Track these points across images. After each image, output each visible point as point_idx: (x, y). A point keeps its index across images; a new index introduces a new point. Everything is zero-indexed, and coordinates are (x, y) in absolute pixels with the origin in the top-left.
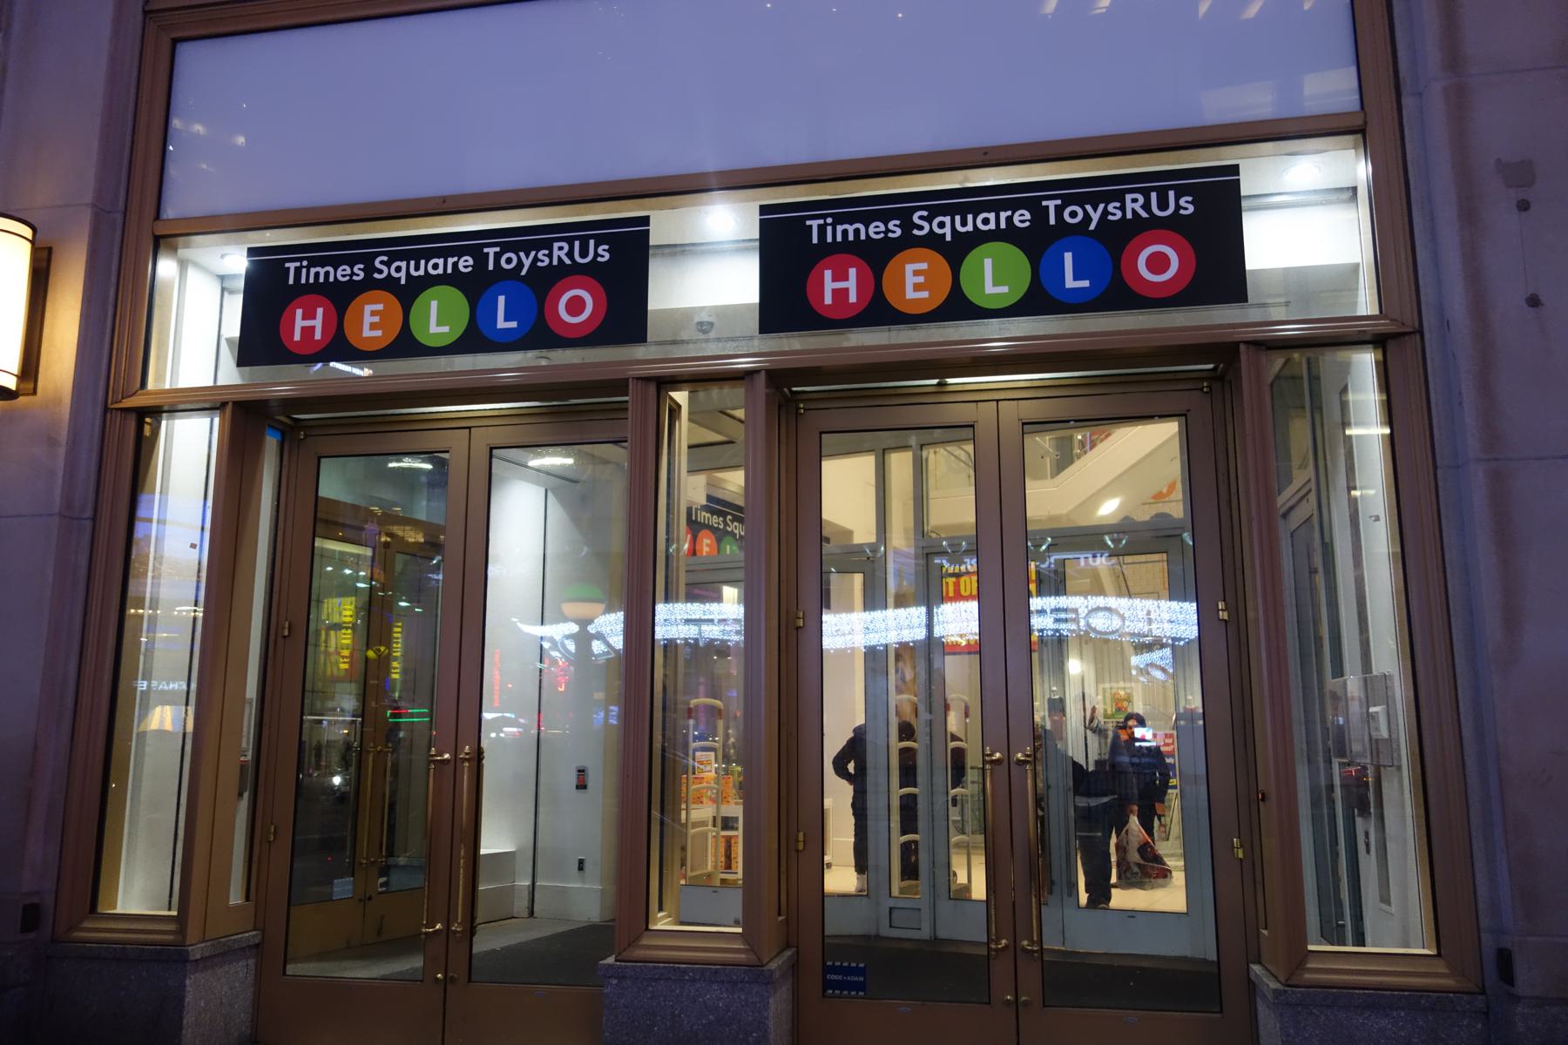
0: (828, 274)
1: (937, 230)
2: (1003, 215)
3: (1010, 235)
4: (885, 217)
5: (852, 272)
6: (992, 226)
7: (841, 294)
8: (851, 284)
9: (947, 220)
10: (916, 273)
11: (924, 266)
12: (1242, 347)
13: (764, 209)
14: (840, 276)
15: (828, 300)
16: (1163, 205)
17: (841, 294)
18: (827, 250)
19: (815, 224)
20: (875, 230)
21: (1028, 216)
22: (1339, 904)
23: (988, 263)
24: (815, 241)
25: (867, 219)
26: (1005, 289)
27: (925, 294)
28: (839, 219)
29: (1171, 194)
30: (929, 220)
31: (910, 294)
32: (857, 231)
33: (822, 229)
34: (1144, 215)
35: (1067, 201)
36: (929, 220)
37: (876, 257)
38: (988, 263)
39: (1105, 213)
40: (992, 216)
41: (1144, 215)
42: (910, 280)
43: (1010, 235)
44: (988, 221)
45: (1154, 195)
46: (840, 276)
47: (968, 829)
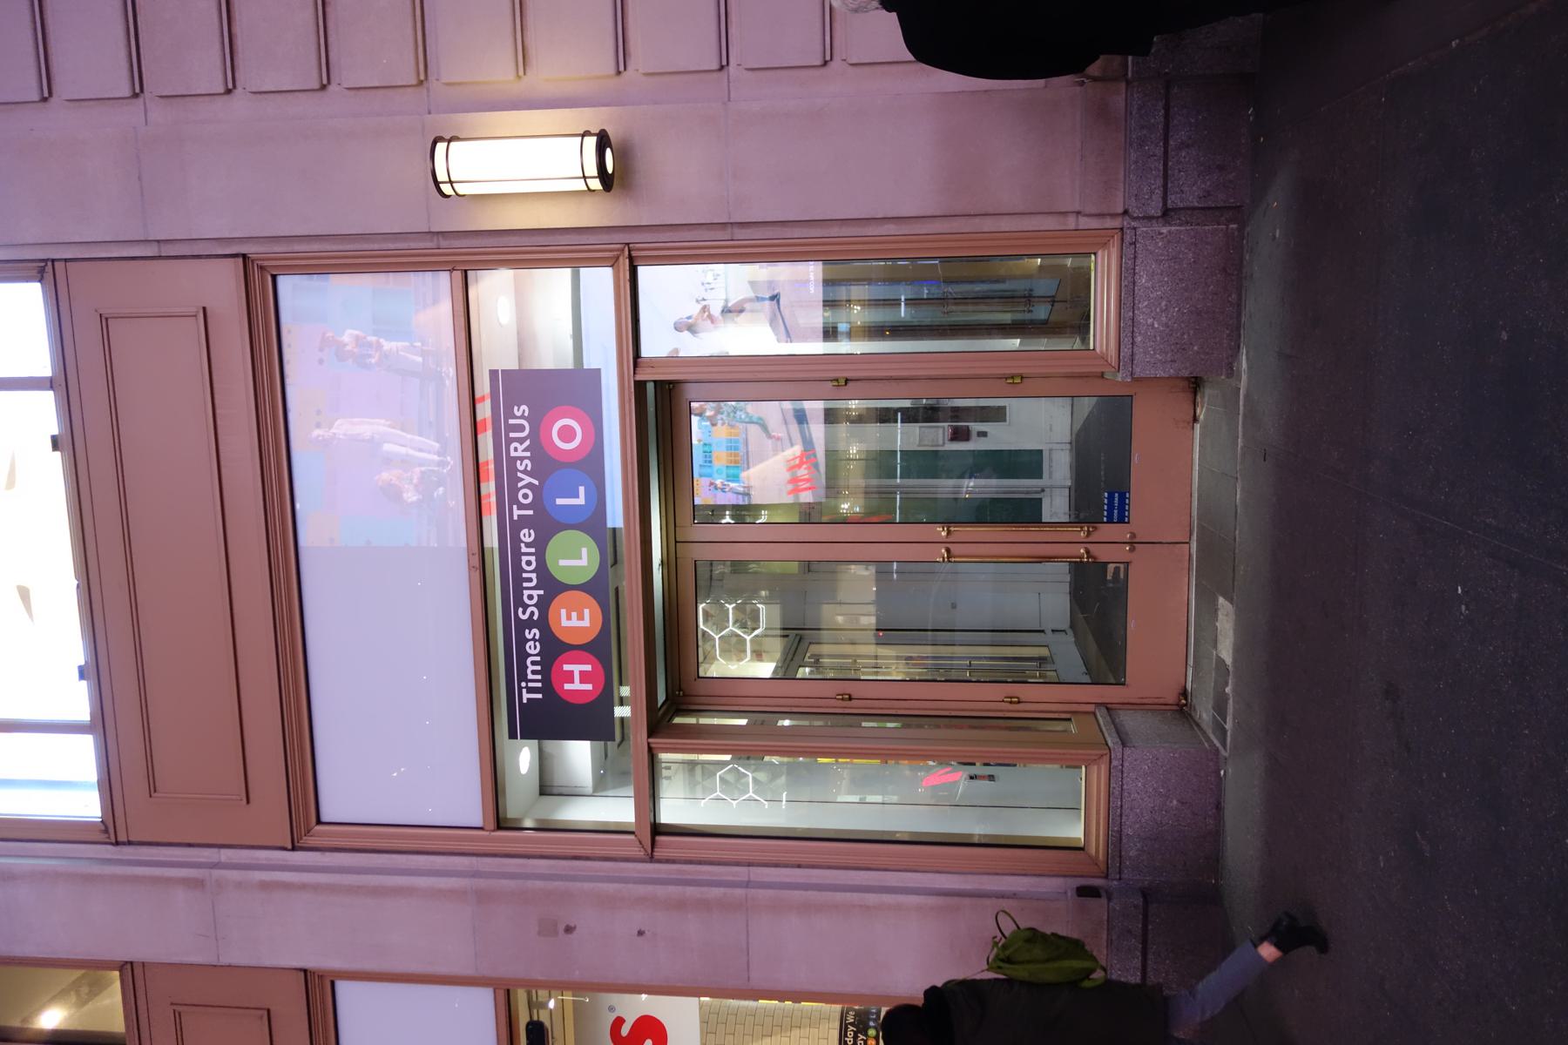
0: (567, 686)
1: (534, 601)
2: (524, 549)
3: (540, 546)
4: (522, 641)
5: (567, 667)
6: (533, 559)
7: (585, 677)
8: (577, 669)
9: (526, 593)
10: (569, 618)
11: (563, 612)
12: (638, 378)
13: (512, 735)
14: (569, 677)
15: (589, 687)
16: (521, 428)
17: (585, 677)
18: (548, 687)
19: (526, 696)
20: (533, 649)
21: (526, 531)
22: (1195, 668)
23: (562, 563)
24: (540, 696)
25: (523, 655)
26: (584, 550)
27: (587, 612)
28: (523, 676)
29: (511, 421)
30: (526, 607)
31: (586, 623)
32: (533, 663)
33: (530, 690)
34: (527, 443)
35: (514, 500)
36: (526, 607)
37: (554, 649)
38: (562, 563)
39: (525, 472)
40: (524, 559)
41: (527, 443)
42: (575, 623)
43: (540, 546)
44: (529, 562)
45: (512, 435)
46: (569, 677)
47: (1112, 876)
